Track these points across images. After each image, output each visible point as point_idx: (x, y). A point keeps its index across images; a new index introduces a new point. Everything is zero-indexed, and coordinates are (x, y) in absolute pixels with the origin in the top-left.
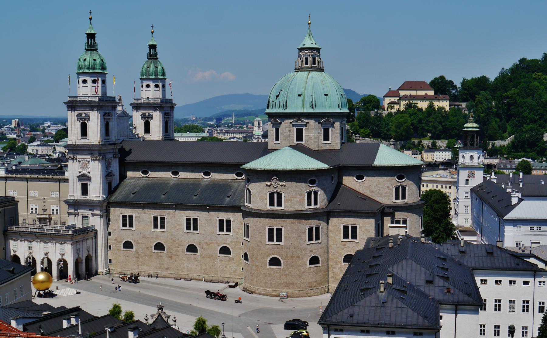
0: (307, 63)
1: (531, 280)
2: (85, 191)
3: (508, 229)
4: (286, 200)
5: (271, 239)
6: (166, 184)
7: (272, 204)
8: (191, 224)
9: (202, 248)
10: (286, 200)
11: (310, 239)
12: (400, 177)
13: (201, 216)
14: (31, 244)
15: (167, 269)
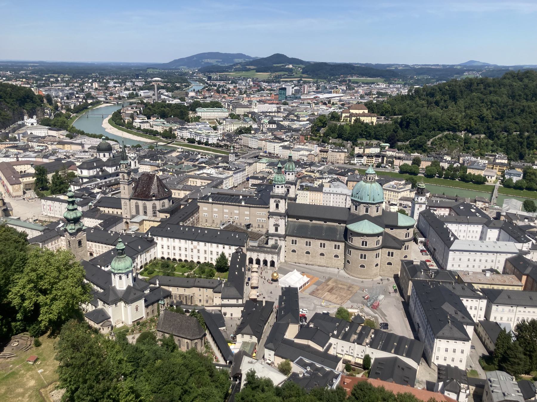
0: (370, 179)
1: (478, 300)
2: (276, 230)
3: (451, 253)
4: (369, 244)
5: (361, 258)
6: (308, 226)
7: (363, 245)
8: (323, 246)
9: (327, 255)
10: (369, 244)
11: (376, 258)
12: (408, 229)
13: (327, 243)
14: (258, 254)
15: (311, 261)
